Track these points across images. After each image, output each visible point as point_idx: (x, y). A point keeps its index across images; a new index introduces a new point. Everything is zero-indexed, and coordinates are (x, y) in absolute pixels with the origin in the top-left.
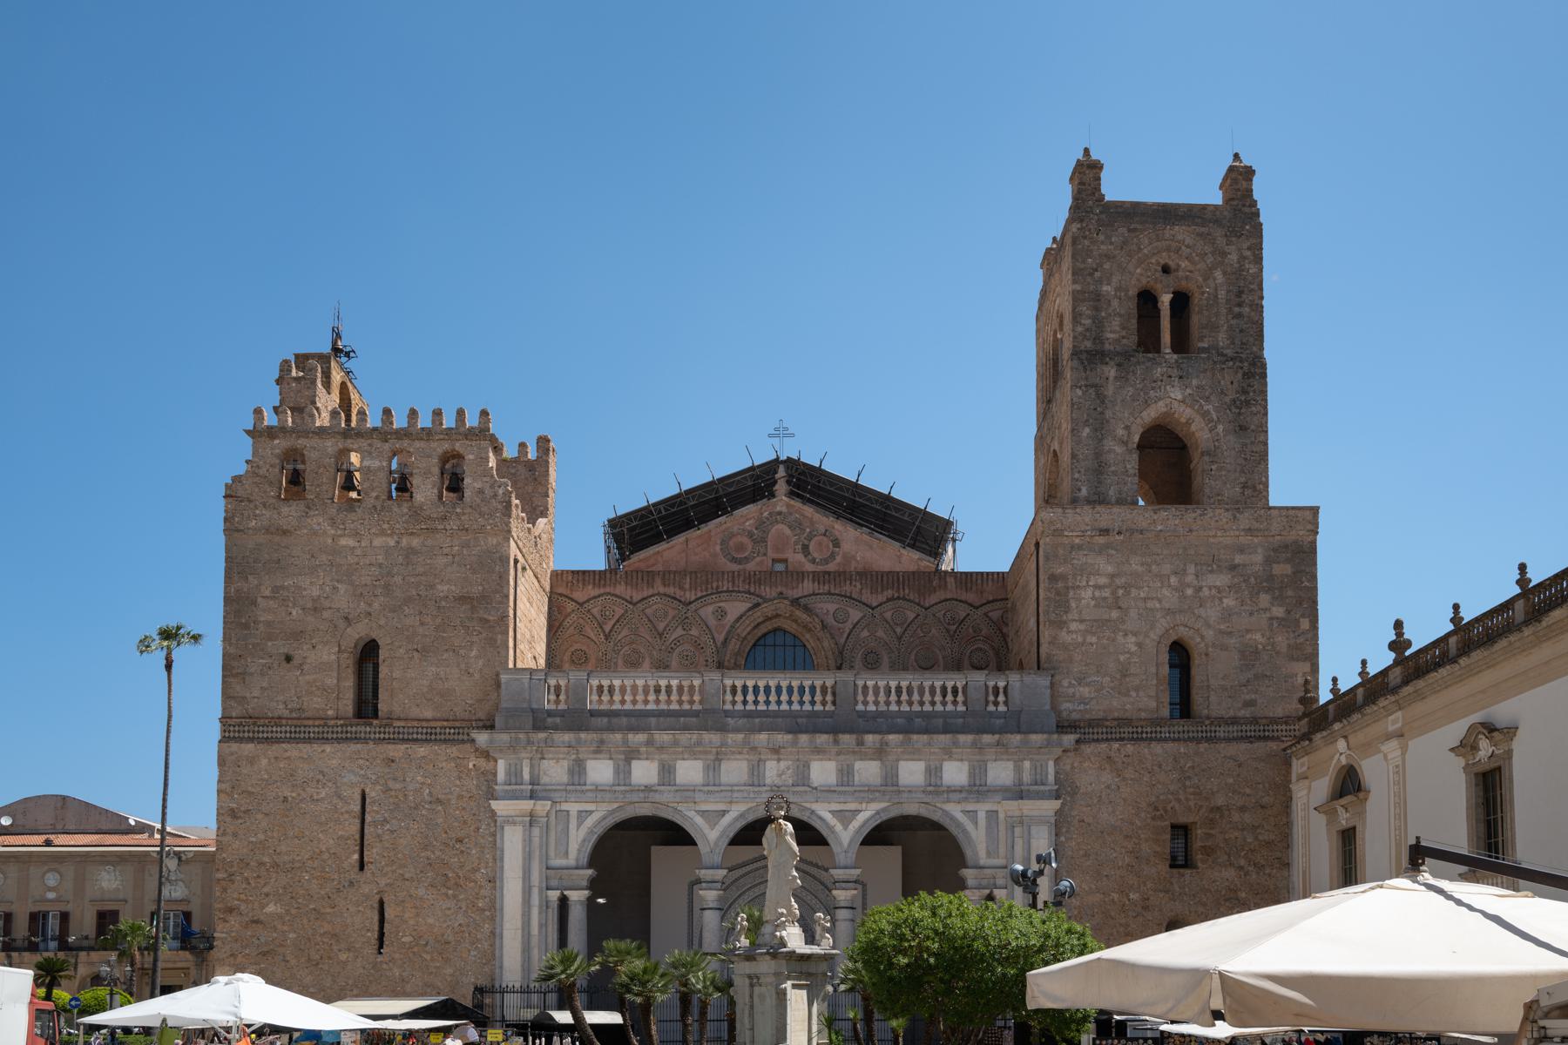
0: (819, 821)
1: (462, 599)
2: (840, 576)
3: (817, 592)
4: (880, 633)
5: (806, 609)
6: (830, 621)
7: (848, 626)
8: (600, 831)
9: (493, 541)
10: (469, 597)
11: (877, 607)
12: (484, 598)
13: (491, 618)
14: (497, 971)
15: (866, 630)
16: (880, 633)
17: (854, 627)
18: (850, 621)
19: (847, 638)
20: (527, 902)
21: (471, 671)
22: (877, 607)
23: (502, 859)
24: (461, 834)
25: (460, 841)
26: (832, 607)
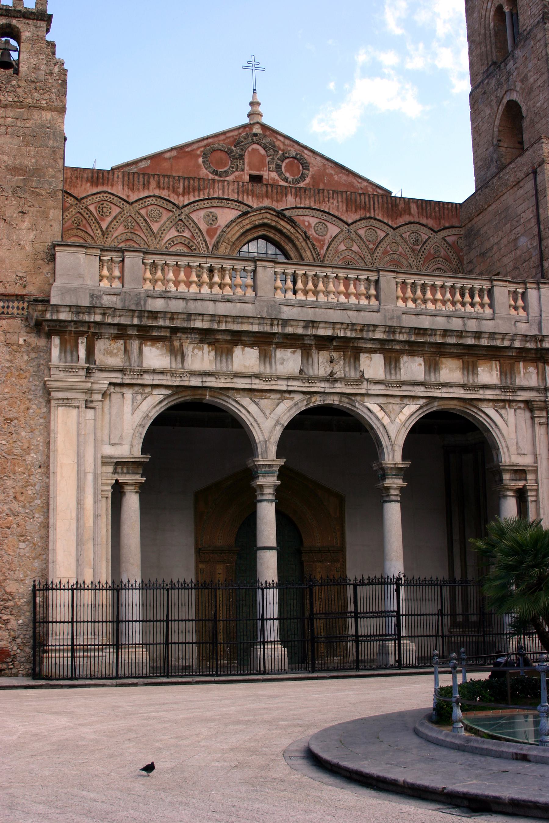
0: (368, 413)
1: (15, 170)
2: (318, 193)
3: (299, 206)
4: (355, 248)
5: (291, 221)
6: (312, 233)
7: (328, 238)
8: (154, 414)
9: (47, 116)
10: (21, 169)
11: (352, 223)
12: (37, 171)
13: (44, 193)
14: (50, 566)
15: (342, 244)
16: (355, 248)
17: (333, 241)
18: (329, 235)
19: (327, 249)
20: (80, 489)
21: (22, 243)
22: (352, 223)
23: (55, 442)
24: (11, 415)
25: (9, 420)
26: (313, 221)
